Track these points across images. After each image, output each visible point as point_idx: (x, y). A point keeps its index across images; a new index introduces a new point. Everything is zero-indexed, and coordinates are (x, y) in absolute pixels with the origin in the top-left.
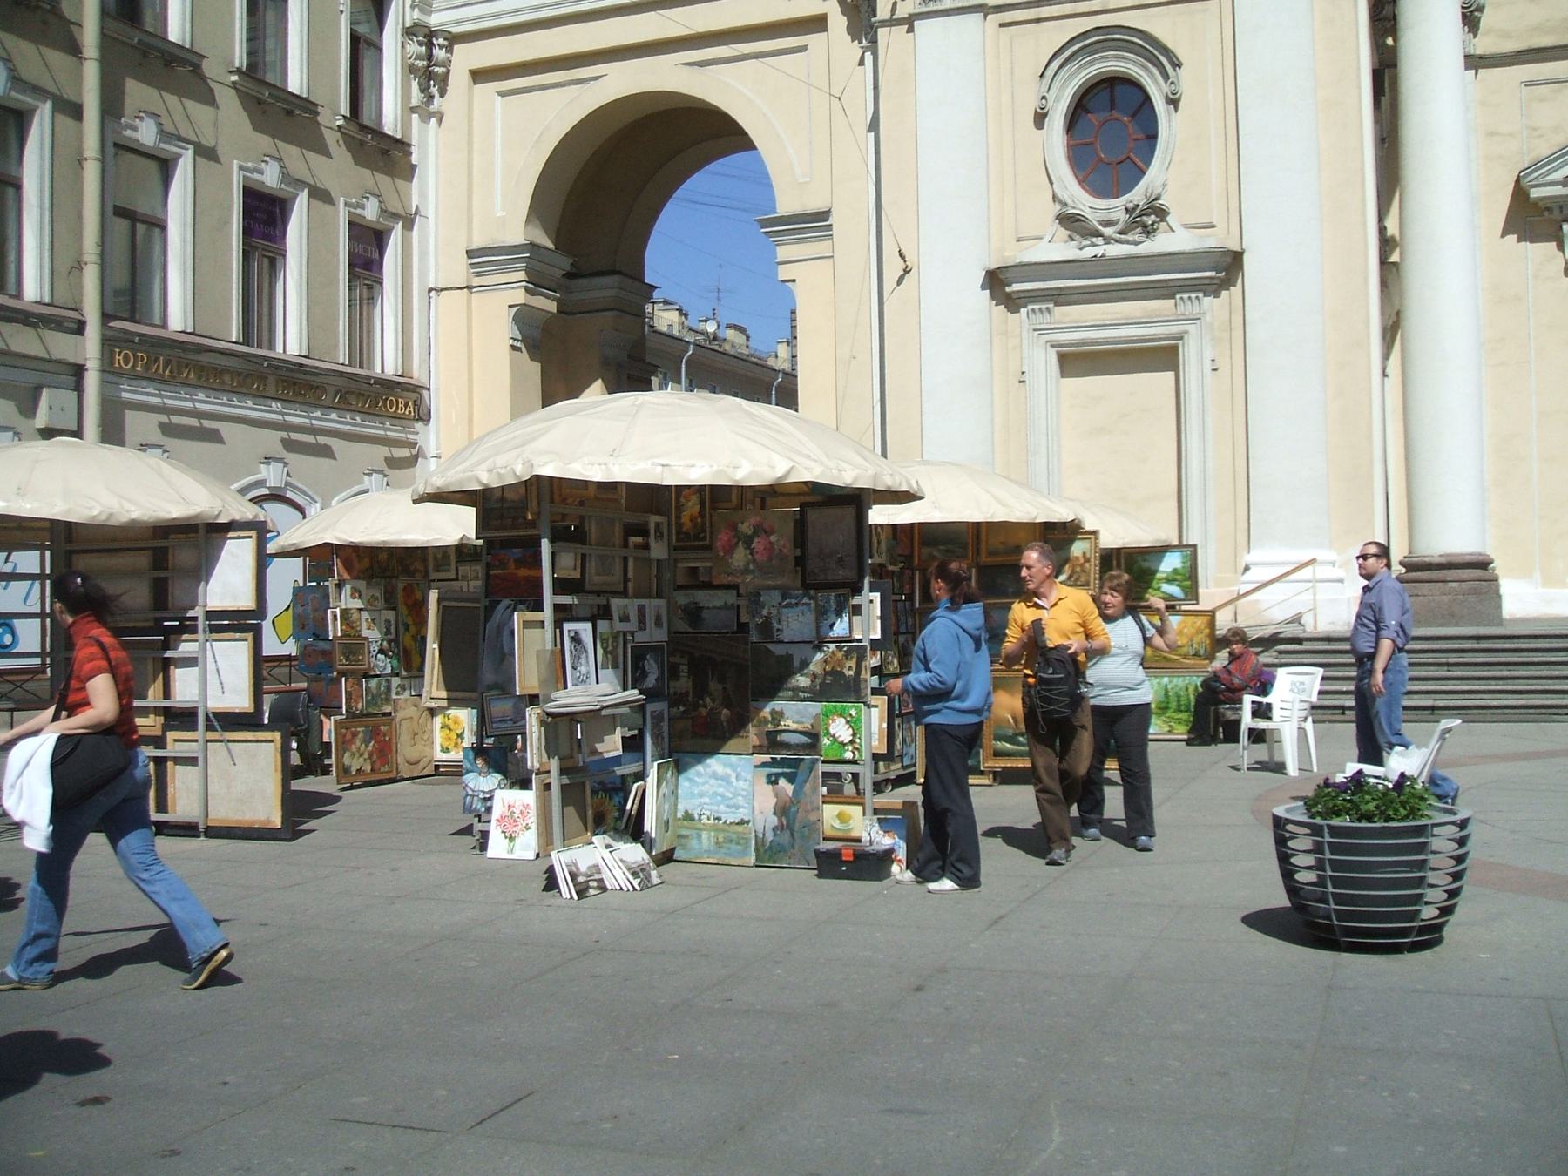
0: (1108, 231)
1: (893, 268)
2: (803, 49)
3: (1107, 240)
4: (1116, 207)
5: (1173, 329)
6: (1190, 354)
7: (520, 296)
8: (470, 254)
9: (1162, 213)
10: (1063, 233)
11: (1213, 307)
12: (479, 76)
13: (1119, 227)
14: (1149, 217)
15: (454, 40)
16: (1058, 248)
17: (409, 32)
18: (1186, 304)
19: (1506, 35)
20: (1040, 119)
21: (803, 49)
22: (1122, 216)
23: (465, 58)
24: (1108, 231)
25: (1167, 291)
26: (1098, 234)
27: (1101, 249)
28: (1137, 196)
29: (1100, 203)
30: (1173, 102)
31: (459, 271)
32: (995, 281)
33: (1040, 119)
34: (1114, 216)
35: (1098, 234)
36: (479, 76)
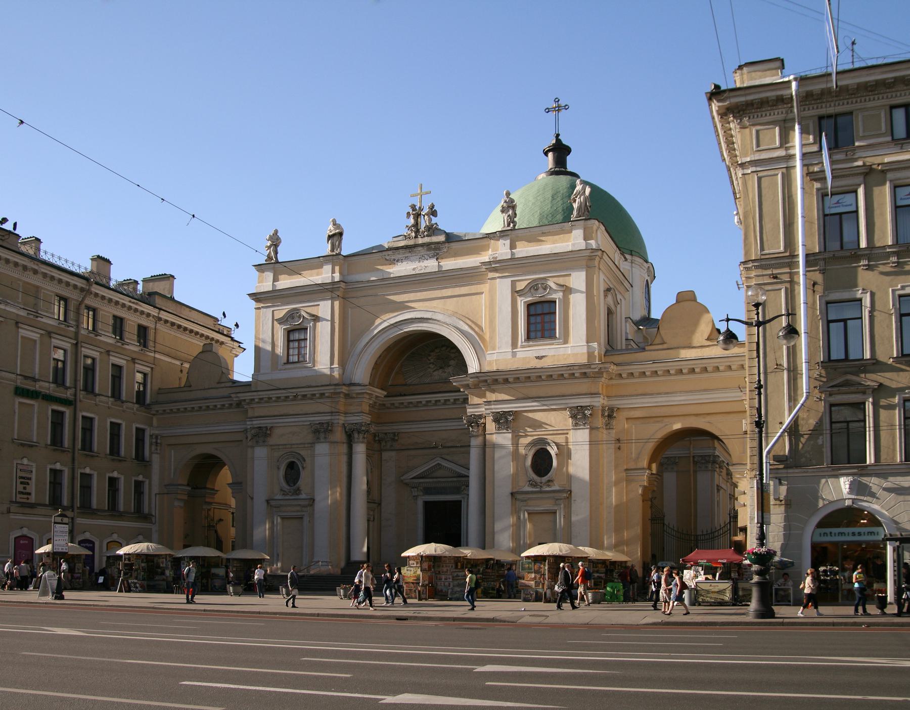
17: (151, 436)
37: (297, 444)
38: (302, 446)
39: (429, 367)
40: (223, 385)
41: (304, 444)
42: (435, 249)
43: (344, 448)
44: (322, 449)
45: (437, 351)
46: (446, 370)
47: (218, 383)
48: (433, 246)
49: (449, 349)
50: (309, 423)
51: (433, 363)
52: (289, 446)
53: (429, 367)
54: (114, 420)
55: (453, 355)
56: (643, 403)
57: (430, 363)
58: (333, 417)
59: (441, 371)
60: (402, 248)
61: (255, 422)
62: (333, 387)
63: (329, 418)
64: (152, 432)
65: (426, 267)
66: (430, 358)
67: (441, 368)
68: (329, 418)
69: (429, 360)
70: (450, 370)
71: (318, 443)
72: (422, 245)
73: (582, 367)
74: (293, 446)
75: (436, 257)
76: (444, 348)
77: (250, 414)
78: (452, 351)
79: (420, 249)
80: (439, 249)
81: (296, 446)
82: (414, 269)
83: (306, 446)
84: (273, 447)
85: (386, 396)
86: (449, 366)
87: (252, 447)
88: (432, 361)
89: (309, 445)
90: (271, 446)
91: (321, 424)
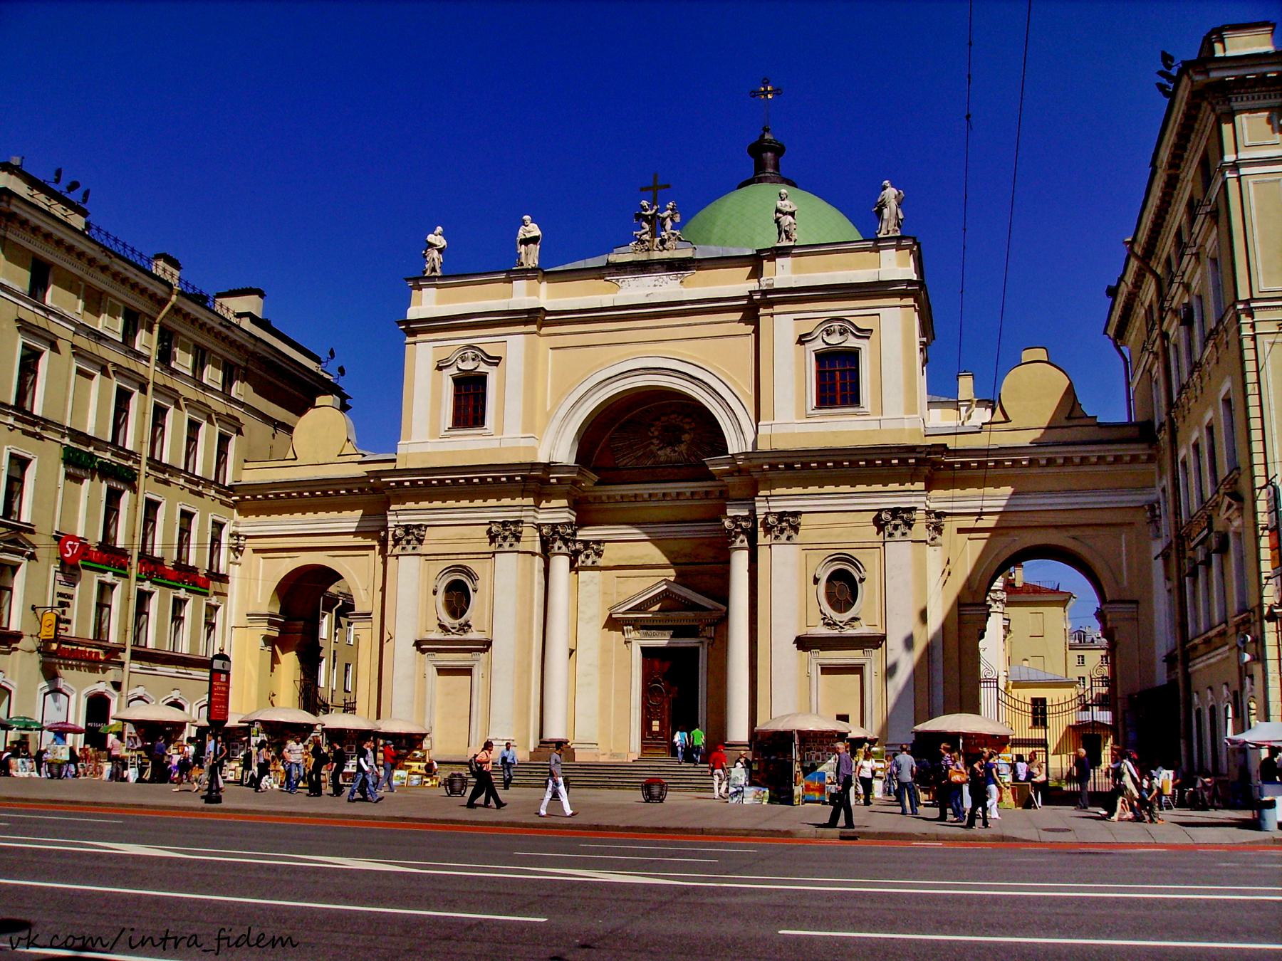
0: (453, 631)
1: (386, 637)
2: (367, 555)
3: (453, 633)
4: (456, 623)
6: (475, 671)
7: (265, 632)
8: (248, 615)
10: (440, 630)
11: (483, 656)
12: (255, 551)
14: (466, 627)
15: (247, 537)
16: (437, 635)
17: (231, 535)
18: (476, 655)
19: (612, 560)
20: (435, 593)
21: (367, 555)
22: (457, 626)
23: (250, 544)
24: (453, 631)
25: (470, 651)
28: (462, 620)
29: (452, 621)
30: (475, 591)
31: (244, 621)
32: (418, 644)
33: (435, 593)
35: (450, 631)
36: (255, 551)
38: (475, 556)
39: (652, 443)
42: (679, 269)
43: (538, 562)
44: (506, 563)
45: (663, 419)
46: (676, 449)
47: (339, 456)
50: (487, 521)
51: (657, 438)
53: (652, 443)
54: (185, 508)
55: (687, 427)
57: (653, 438)
58: (523, 514)
61: (400, 518)
63: (518, 514)
64: (234, 529)
66: (652, 429)
68: (518, 514)
69: (652, 433)
70: (683, 447)
74: (460, 557)
78: (687, 420)
81: (465, 556)
84: (428, 558)
85: (596, 484)
86: (682, 442)
87: (397, 556)
88: (656, 433)
91: (504, 524)
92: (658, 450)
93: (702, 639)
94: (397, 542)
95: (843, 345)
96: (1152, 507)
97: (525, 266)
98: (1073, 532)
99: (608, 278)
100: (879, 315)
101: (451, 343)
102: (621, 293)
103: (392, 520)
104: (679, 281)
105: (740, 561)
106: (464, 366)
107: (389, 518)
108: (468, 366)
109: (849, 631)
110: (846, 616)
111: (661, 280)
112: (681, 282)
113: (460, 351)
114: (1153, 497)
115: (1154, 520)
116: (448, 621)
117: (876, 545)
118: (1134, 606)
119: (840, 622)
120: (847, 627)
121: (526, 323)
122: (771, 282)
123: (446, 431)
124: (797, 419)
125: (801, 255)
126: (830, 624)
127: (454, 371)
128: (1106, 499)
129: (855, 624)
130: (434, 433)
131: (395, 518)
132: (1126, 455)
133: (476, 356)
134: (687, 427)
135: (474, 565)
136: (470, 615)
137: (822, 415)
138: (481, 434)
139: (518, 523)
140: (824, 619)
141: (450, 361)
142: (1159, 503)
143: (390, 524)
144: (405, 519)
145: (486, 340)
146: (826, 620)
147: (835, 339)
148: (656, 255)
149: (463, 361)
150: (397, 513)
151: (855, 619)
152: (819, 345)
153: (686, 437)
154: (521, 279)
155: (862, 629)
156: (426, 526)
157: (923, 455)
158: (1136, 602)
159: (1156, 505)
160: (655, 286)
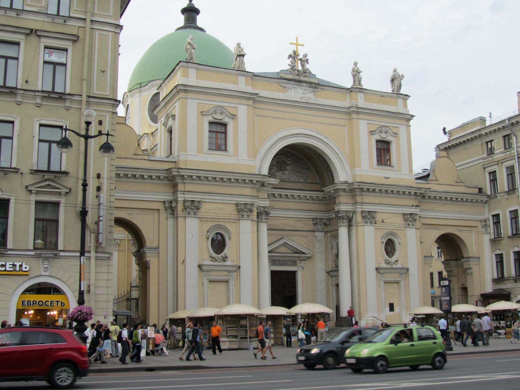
0: (218, 260)
3: (219, 262)
5: (228, 278)
9: (227, 258)
11: (234, 274)
13: (220, 260)
14: (225, 259)
24: (218, 260)
26: (217, 261)
27: (216, 263)
28: (223, 254)
30: (230, 239)
34: (219, 258)
35: (217, 261)
37: (223, 219)
38: (228, 221)
39: (273, 168)
40: (140, 157)
41: (230, 219)
42: (314, 88)
46: (284, 173)
48: (314, 85)
49: (286, 157)
50: (236, 203)
52: (217, 220)
53: (273, 168)
55: (289, 162)
56: (438, 216)
59: (281, 172)
60: (290, 80)
61: (186, 196)
62: (262, 177)
63: (250, 200)
65: (309, 99)
67: (281, 170)
68: (250, 200)
70: (287, 172)
71: (242, 219)
72: (306, 82)
73: (417, 189)
74: (220, 220)
75: (313, 94)
76: (283, 156)
77: (181, 187)
79: (305, 84)
80: (316, 88)
81: (222, 220)
82: (301, 98)
83: (231, 221)
84: (202, 219)
86: (287, 170)
89: (234, 221)
90: (200, 218)
92: (276, 172)
93: (299, 268)
94: (185, 208)
95: (386, 138)
96: (485, 221)
97: (241, 69)
98: (459, 228)
99: (281, 85)
100: (398, 127)
101: (212, 103)
102: (287, 94)
103: (181, 197)
104: (313, 94)
105: (343, 231)
106: (215, 116)
107: (179, 195)
108: (218, 117)
109: (394, 266)
110: (393, 259)
111: (306, 92)
112: (314, 95)
113: (214, 108)
114: (484, 217)
115: (486, 226)
116: (214, 255)
117: (402, 229)
118: (478, 259)
119: (392, 262)
120: (394, 265)
121: (248, 99)
122: (357, 104)
123: (207, 151)
124: (370, 169)
125: (367, 94)
126: (387, 263)
127: (211, 119)
128: (457, 216)
129: (396, 263)
130: (200, 150)
131: (183, 196)
132: (479, 200)
133: (223, 112)
134: (289, 162)
135: (228, 226)
136: (226, 251)
137: (379, 169)
138: (226, 155)
139: (252, 205)
140: (385, 260)
141: (209, 112)
142: (489, 220)
143: (179, 199)
144: (189, 197)
145: (227, 104)
146: (386, 261)
147: (383, 135)
148: (302, 78)
149: (216, 114)
150: (184, 192)
151: (397, 261)
152: (377, 137)
153: (288, 167)
154: (244, 75)
155: (399, 265)
156: (203, 202)
157: (423, 192)
158: (479, 258)
159: (488, 221)
160: (303, 93)
